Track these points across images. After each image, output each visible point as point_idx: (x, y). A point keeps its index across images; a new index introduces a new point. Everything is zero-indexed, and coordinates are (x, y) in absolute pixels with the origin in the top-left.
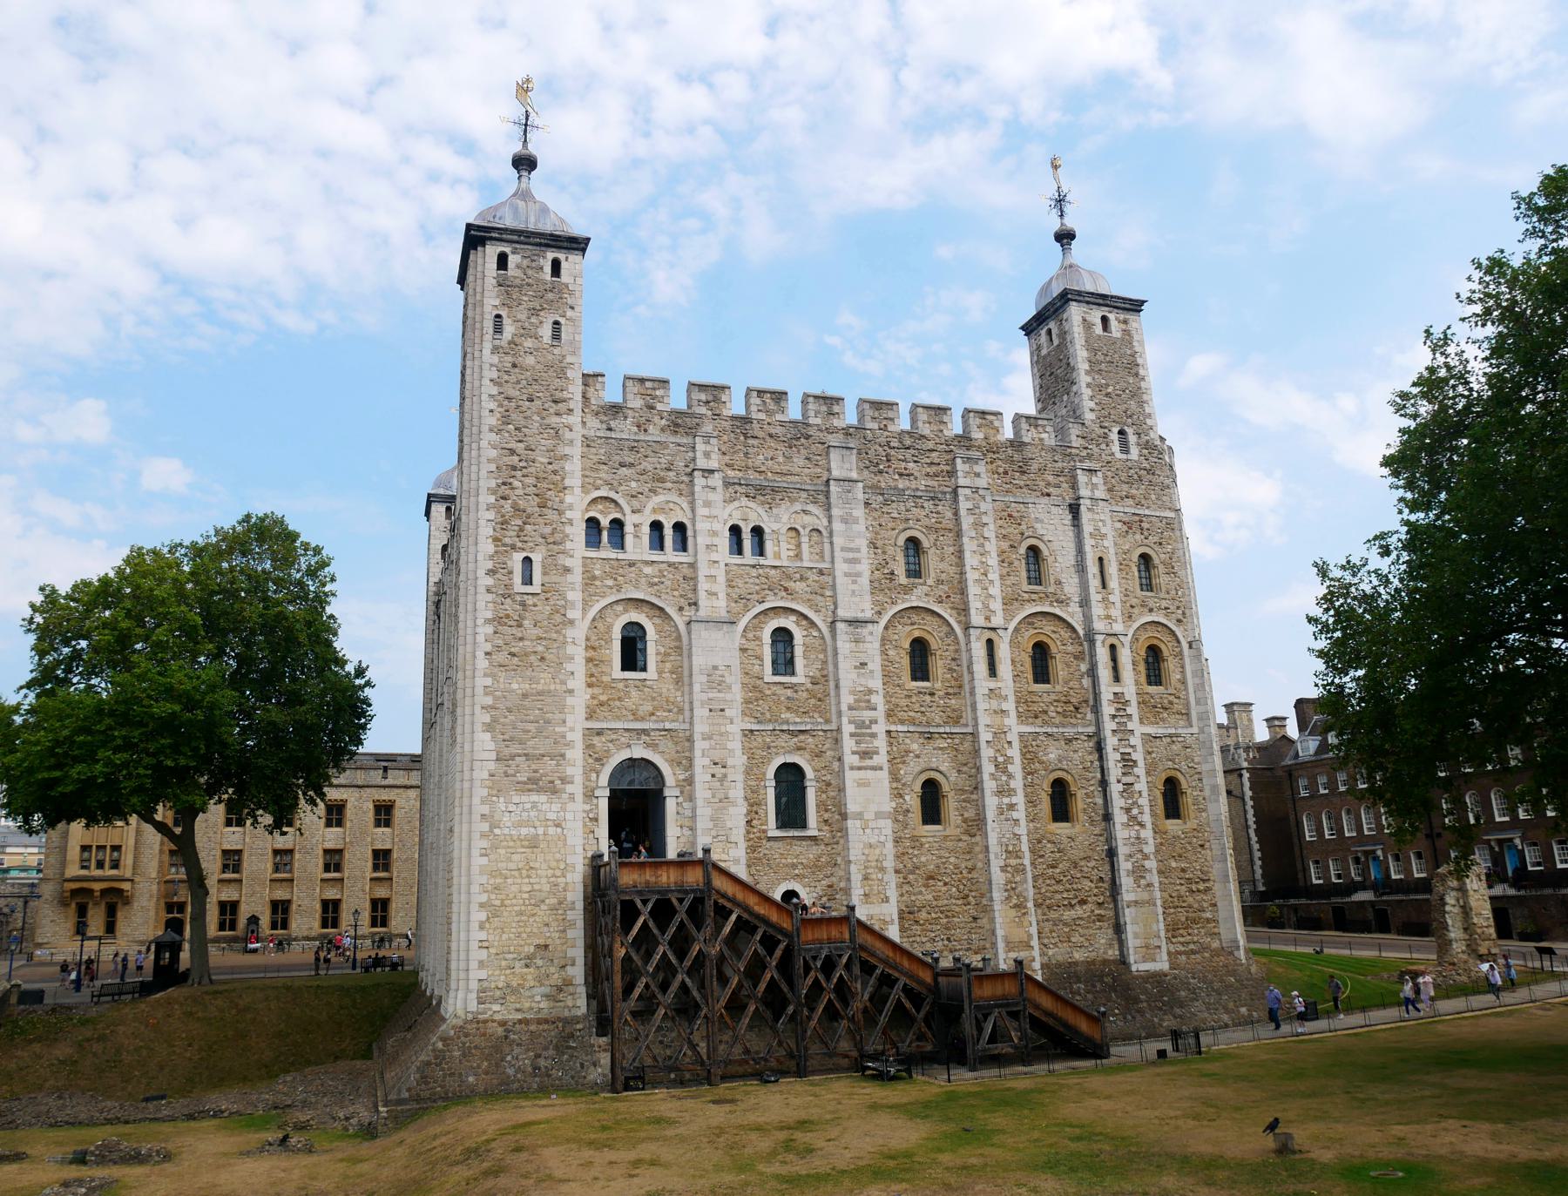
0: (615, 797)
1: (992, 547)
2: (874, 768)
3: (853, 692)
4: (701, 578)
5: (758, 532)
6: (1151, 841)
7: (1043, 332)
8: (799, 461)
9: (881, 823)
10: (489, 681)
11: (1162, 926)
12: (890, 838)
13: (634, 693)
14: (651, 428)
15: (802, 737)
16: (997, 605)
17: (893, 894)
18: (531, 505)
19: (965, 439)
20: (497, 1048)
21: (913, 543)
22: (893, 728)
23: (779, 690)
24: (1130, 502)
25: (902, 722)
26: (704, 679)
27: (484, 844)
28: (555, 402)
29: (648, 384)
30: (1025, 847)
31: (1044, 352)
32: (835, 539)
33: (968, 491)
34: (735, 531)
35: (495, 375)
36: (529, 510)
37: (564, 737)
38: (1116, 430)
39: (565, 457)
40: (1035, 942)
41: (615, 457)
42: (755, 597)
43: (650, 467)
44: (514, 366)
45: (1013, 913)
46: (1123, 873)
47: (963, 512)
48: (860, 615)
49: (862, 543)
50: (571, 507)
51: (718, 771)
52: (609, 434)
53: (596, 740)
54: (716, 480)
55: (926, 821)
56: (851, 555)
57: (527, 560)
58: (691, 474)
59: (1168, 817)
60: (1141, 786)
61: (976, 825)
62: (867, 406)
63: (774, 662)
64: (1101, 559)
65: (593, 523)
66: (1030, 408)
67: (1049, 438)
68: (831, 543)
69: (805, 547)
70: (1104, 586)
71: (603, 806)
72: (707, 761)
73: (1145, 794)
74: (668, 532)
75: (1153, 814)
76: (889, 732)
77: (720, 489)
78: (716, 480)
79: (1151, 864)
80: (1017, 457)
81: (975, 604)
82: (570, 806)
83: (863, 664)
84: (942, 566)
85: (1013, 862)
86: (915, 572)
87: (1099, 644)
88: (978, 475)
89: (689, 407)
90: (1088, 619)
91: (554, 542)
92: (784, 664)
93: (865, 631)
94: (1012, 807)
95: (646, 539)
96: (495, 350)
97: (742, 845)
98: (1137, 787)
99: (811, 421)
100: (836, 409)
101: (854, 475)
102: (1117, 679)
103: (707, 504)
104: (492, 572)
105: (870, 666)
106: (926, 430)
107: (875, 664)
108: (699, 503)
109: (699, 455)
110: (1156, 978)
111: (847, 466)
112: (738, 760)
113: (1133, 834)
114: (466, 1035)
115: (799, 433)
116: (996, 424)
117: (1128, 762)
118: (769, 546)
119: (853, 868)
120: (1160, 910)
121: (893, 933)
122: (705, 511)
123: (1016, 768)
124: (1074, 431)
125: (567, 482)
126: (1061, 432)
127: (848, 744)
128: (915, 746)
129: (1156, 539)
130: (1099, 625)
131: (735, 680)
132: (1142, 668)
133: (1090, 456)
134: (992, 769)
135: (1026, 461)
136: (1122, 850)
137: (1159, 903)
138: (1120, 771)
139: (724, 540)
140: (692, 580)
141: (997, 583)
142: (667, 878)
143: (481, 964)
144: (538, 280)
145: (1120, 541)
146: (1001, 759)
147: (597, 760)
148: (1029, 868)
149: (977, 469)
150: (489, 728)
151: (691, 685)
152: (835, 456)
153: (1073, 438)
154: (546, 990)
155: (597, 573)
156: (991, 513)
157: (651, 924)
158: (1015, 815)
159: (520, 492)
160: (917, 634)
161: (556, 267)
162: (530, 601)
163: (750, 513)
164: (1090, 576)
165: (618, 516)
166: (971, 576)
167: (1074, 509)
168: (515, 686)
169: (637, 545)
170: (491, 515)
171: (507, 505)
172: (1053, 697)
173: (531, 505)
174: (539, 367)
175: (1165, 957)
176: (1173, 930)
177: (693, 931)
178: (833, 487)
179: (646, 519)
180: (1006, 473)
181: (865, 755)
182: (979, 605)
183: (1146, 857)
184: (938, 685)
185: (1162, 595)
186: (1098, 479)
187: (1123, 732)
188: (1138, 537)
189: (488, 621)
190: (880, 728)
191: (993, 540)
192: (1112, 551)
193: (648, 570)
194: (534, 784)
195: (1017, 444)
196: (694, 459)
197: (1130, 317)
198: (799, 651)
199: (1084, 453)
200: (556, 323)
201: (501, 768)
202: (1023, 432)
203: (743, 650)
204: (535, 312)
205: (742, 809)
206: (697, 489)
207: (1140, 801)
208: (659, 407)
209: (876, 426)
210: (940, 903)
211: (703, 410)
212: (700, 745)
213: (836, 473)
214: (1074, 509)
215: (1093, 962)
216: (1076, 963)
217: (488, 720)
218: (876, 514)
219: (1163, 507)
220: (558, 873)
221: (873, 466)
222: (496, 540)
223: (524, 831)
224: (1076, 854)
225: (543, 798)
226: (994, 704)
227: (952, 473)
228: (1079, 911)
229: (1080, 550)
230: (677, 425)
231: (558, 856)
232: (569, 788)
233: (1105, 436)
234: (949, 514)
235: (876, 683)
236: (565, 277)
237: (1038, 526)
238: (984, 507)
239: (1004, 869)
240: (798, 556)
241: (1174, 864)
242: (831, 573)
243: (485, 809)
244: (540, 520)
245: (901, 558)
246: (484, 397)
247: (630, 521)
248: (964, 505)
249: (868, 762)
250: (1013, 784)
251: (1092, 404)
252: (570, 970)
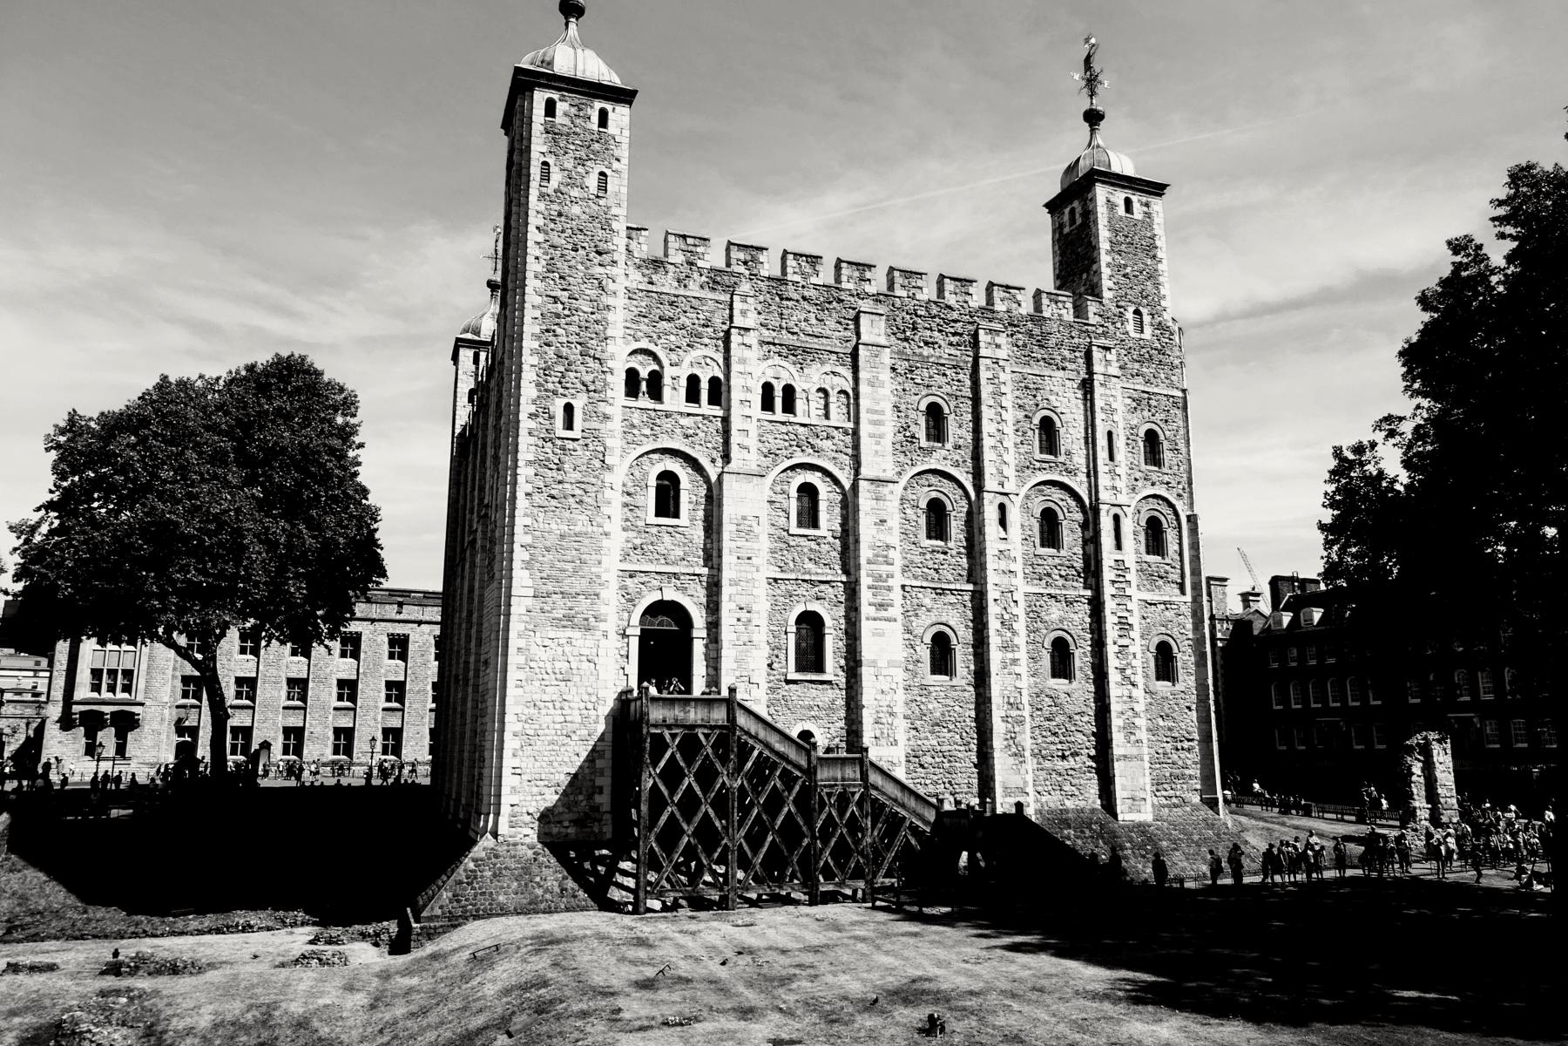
0: (645, 637)
1: (1011, 415)
2: (888, 620)
3: (873, 547)
4: (734, 432)
5: (789, 391)
6: (1142, 700)
7: (1067, 211)
8: (831, 323)
9: (893, 671)
10: (528, 521)
11: (1148, 779)
12: (901, 686)
13: (667, 538)
14: (691, 285)
15: (823, 587)
16: (1010, 472)
17: (902, 737)
18: (574, 353)
19: (988, 309)
20: (526, 870)
22: (907, 582)
23: (803, 541)
24: (1140, 379)
25: (916, 577)
26: (734, 528)
27: (521, 675)
28: (600, 253)
29: (690, 241)
30: (1025, 699)
31: (1066, 230)
32: (862, 401)
33: (988, 361)
34: (768, 389)
35: (541, 222)
36: (572, 358)
37: (599, 577)
38: (1131, 309)
39: (608, 307)
40: (1030, 789)
41: (658, 310)
42: (784, 452)
43: (688, 323)
44: (560, 214)
45: (1011, 760)
46: (1114, 729)
47: (983, 381)
48: (882, 476)
49: (887, 407)
50: (612, 357)
51: (744, 615)
52: (650, 287)
53: (629, 581)
54: (752, 338)
55: (933, 672)
56: (876, 417)
57: (569, 409)
58: (728, 334)
59: (1158, 679)
60: (1136, 648)
61: (981, 678)
62: (896, 274)
63: (799, 514)
64: (1110, 434)
65: (632, 375)
66: (1048, 284)
67: (1069, 316)
68: (857, 405)
69: (833, 407)
70: (1111, 458)
71: (634, 643)
72: (733, 606)
73: (1139, 655)
74: (704, 386)
75: (1146, 676)
76: (903, 587)
77: (755, 345)
79: (1141, 722)
80: (1037, 331)
81: (989, 469)
82: (603, 642)
83: (883, 521)
84: (963, 432)
85: (1014, 713)
87: (1103, 513)
88: (998, 346)
89: (728, 265)
90: (1094, 489)
92: (810, 516)
93: (885, 490)
94: (1015, 661)
95: (683, 392)
96: (542, 196)
97: (764, 686)
98: (1131, 649)
99: (844, 285)
100: (868, 275)
101: (883, 341)
102: (1119, 546)
103: (743, 361)
104: (532, 416)
105: (889, 523)
106: (951, 300)
107: (895, 521)
108: (734, 360)
109: (736, 312)
110: (1141, 828)
111: (876, 331)
112: (762, 606)
113: (1126, 693)
114: (496, 856)
115: (832, 296)
116: (1019, 297)
117: (1124, 625)
118: (800, 405)
119: (865, 711)
120: (1147, 765)
121: (900, 773)
122: (740, 368)
123: (1020, 626)
124: (1092, 307)
125: (609, 333)
126: (1080, 311)
127: (865, 596)
128: (927, 601)
129: (1163, 416)
130: (1104, 495)
131: (763, 530)
132: (1142, 537)
133: (1104, 334)
134: (999, 626)
135: (1045, 335)
136: (1115, 707)
137: (1146, 758)
138: (1116, 633)
140: (726, 433)
141: (1012, 450)
142: (694, 715)
143: (514, 790)
144: (585, 129)
145: (1129, 416)
146: (1006, 617)
147: (631, 600)
148: (1028, 719)
149: (998, 340)
150: (528, 565)
151: (719, 533)
152: (864, 320)
153: (1091, 315)
154: (575, 816)
155: (636, 422)
156: (1009, 383)
157: (678, 756)
158: (1017, 669)
159: (564, 339)
160: (934, 495)
161: (603, 117)
162: (570, 445)
163: (783, 373)
164: (1099, 448)
165: (656, 367)
166: (987, 442)
167: (1087, 387)
168: (554, 526)
169: (674, 397)
170: (535, 360)
171: (551, 351)
172: (1057, 561)
173: (574, 353)
174: (583, 217)
175: (1149, 808)
176: (1158, 784)
177: (718, 766)
178: (862, 351)
179: (684, 372)
180: (1025, 345)
181: (881, 606)
182: (994, 471)
183: (1136, 715)
184: (951, 544)
185: (1165, 470)
186: (1112, 356)
187: (1122, 596)
188: (1146, 413)
189: (530, 463)
190: (896, 582)
191: (1010, 409)
192: (1121, 425)
193: (685, 421)
194: (569, 620)
195: (1037, 317)
196: (731, 317)
197: (1153, 200)
198: (823, 506)
199: (1100, 330)
200: (602, 174)
201: (538, 604)
202: (1044, 307)
203: (771, 502)
204: (581, 162)
205: (766, 650)
206: (733, 346)
207: (1134, 663)
208: (700, 263)
209: (904, 293)
210: (944, 748)
211: (742, 269)
212: (727, 590)
214: (1087, 387)
215: (1082, 811)
216: (1067, 811)
217: (527, 557)
218: (900, 379)
219: (1173, 386)
220: (590, 706)
221: (903, 332)
222: (538, 385)
223: (558, 665)
224: (1070, 709)
225: (576, 634)
226: (1003, 565)
227: (975, 344)
228: (1071, 762)
229: (1090, 425)
230: (715, 282)
231: (590, 690)
232: (602, 626)
233: (1121, 315)
234: (968, 383)
235: (894, 539)
236: (612, 129)
237: (1053, 398)
238: (1003, 377)
239: (1005, 719)
240: (827, 416)
241: (1161, 723)
242: (856, 433)
243: (522, 643)
244: (582, 368)
245: (922, 421)
246: (530, 244)
247: (668, 373)
248: (984, 375)
249: (883, 614)
250: (1017, 640)
251: (1110, 284)
252: (598, 799)
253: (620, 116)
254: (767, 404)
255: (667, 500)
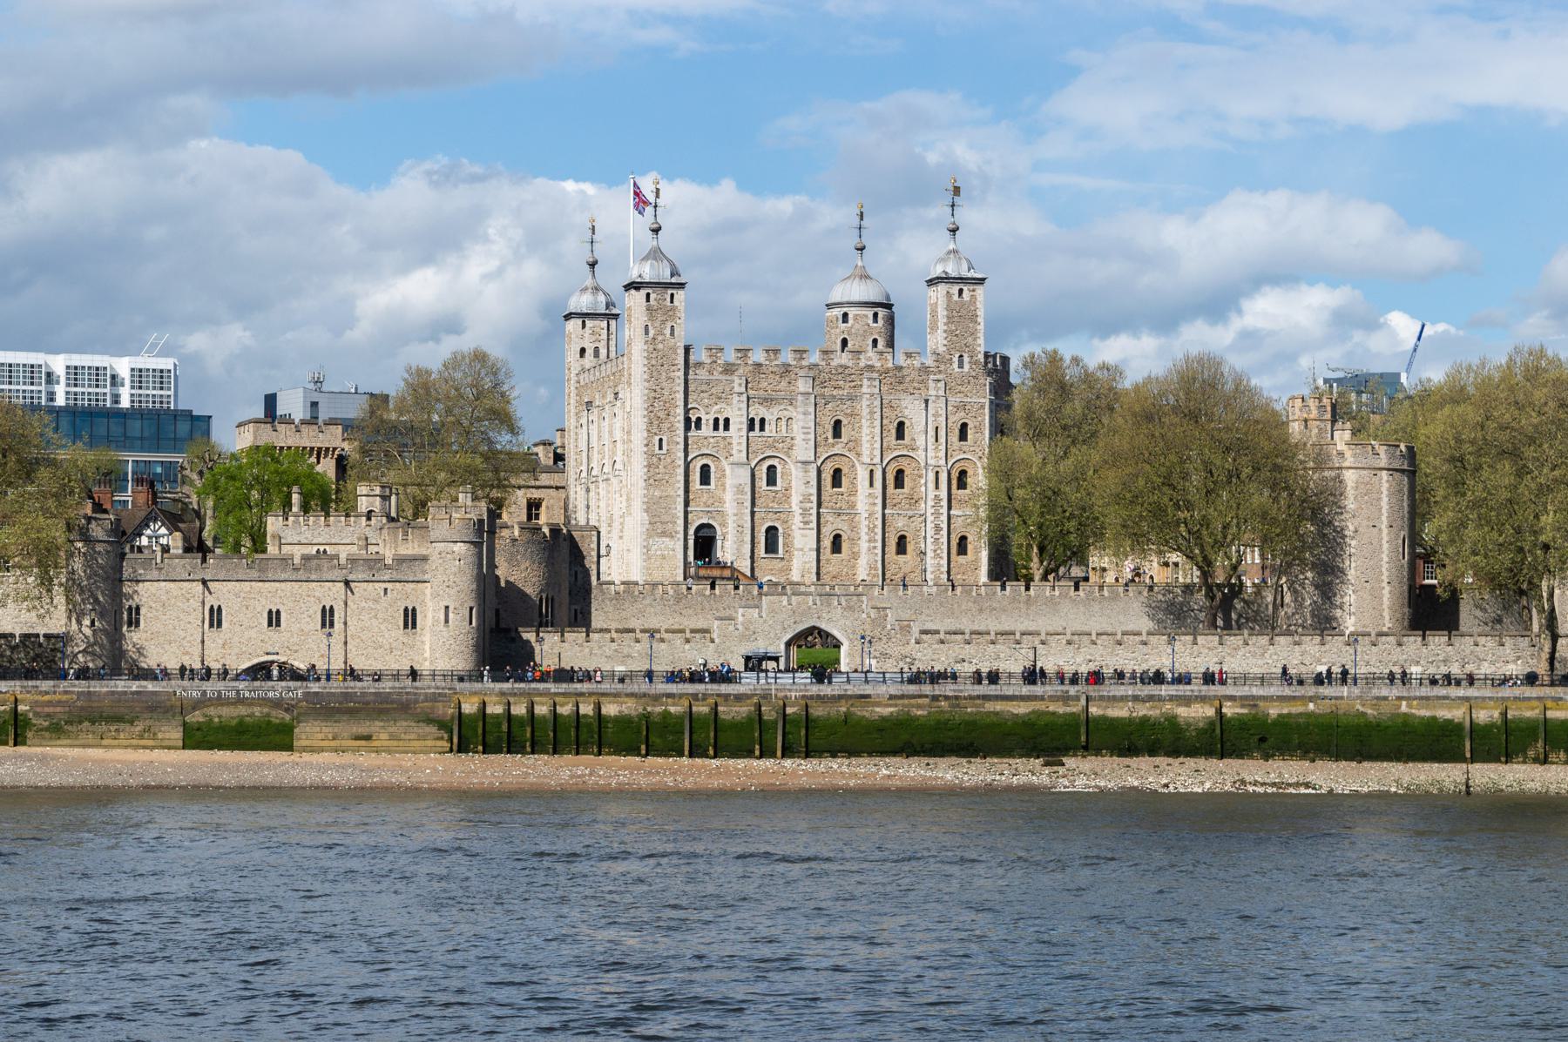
5: (763, 421)
16: (877, 453)
21: (838, 424)
65: (687, 420)
74: (721, 423)
78: (744, 398)
86: (837, 433)
91: (671, 429)
107: (814, 483)
123: (879, 530)
136: (929, 569)
139: (745, 427)
163: (758, 412)
166: (865, 439)
169: (707, 429)
178: (800, 398)
179: (711, 418)
213: (802, 389)
235: (814, 491)
253: (680, 295)
254: (751, 427)
255: (705, 480)
